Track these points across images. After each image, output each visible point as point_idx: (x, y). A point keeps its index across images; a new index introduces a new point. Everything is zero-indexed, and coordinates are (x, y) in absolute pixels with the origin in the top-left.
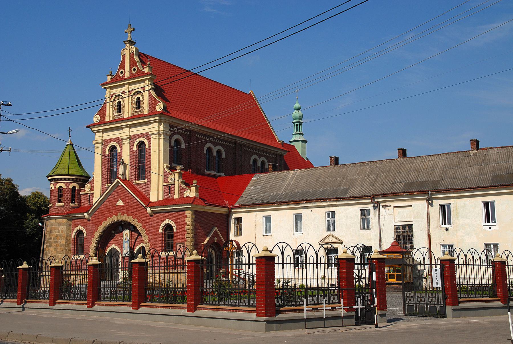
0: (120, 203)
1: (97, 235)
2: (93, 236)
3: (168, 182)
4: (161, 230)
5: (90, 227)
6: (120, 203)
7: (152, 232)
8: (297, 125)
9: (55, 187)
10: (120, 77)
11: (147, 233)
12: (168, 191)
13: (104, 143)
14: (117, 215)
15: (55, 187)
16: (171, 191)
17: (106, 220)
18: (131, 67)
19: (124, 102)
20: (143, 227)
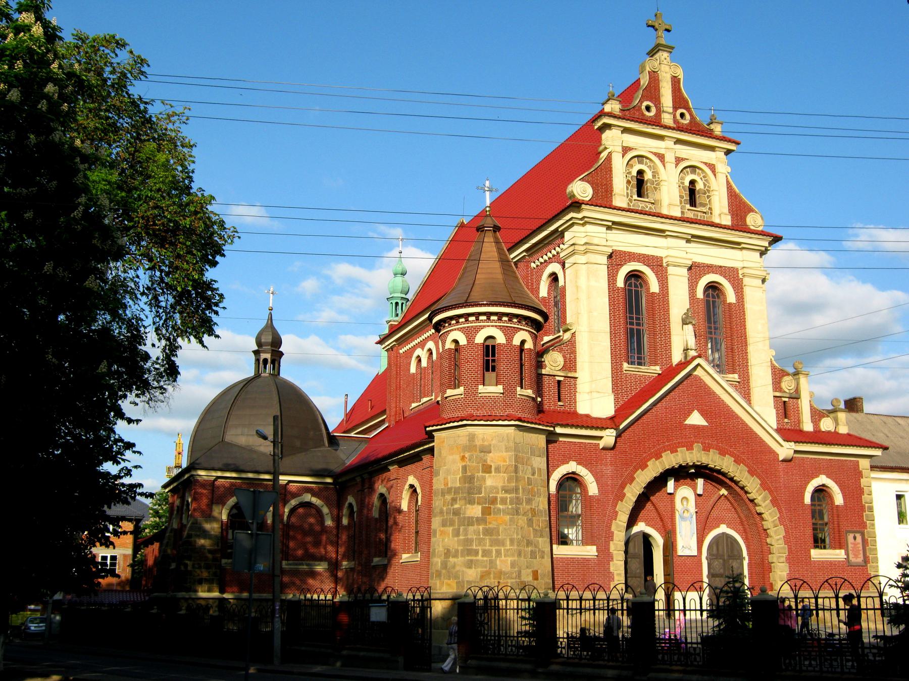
0: (696, 419)
1: (632, 492)
2: (621, 497)
3: (781, 390)
4: (807, 499)
5: (608, 470)
6: (696, 419)
7: (787, 502)
8: (397, 304)
9: (509, 339)
10: (643, 115)
11: (774, 502)
12: (782, 411)
13: (615, 259)
14: (690, 448)
15: (509, 339)
16: (791, 412)
17: (658, 456)
18: (675, 108)
19: (655, 174)
20: (764, 486)
